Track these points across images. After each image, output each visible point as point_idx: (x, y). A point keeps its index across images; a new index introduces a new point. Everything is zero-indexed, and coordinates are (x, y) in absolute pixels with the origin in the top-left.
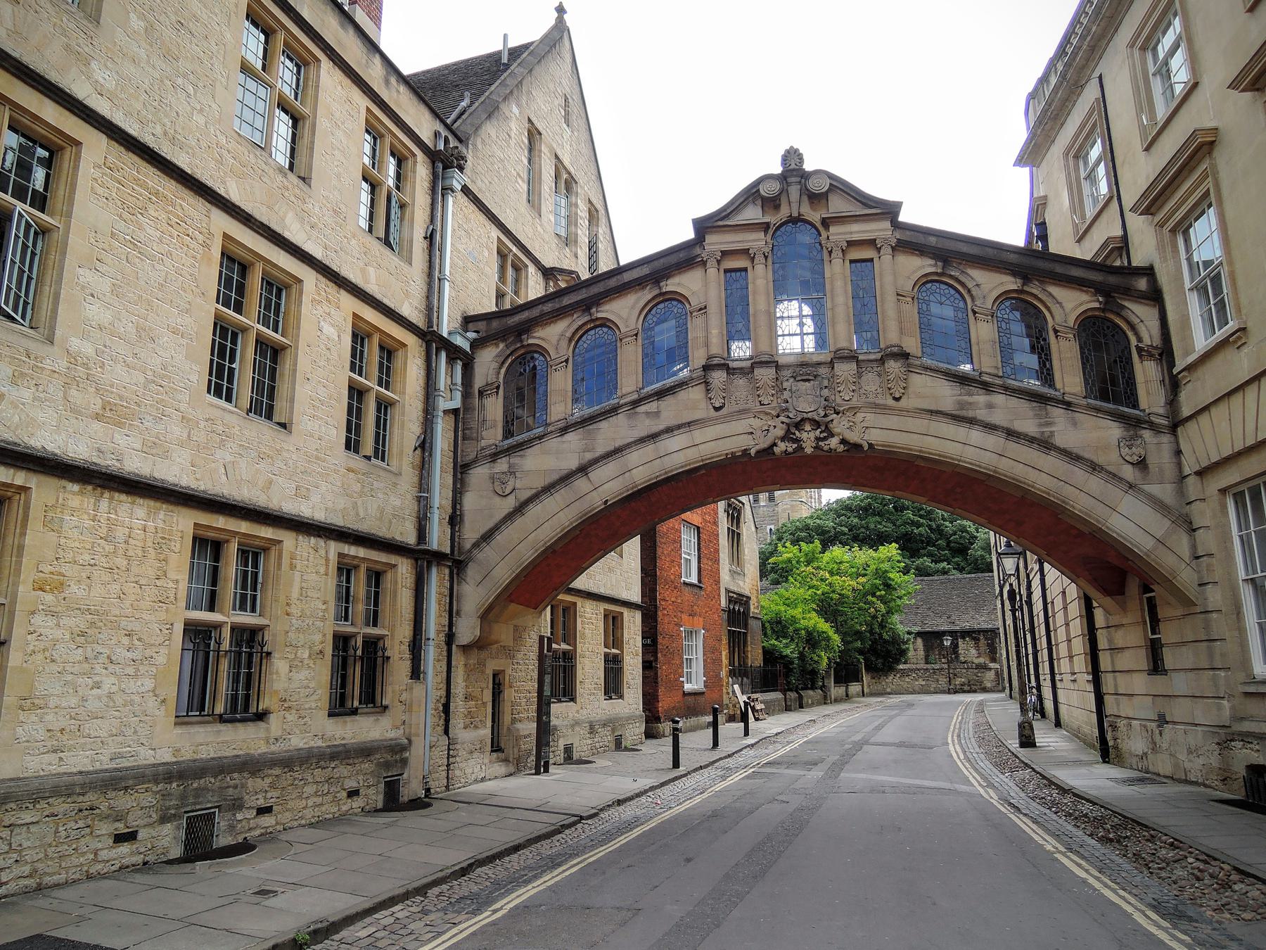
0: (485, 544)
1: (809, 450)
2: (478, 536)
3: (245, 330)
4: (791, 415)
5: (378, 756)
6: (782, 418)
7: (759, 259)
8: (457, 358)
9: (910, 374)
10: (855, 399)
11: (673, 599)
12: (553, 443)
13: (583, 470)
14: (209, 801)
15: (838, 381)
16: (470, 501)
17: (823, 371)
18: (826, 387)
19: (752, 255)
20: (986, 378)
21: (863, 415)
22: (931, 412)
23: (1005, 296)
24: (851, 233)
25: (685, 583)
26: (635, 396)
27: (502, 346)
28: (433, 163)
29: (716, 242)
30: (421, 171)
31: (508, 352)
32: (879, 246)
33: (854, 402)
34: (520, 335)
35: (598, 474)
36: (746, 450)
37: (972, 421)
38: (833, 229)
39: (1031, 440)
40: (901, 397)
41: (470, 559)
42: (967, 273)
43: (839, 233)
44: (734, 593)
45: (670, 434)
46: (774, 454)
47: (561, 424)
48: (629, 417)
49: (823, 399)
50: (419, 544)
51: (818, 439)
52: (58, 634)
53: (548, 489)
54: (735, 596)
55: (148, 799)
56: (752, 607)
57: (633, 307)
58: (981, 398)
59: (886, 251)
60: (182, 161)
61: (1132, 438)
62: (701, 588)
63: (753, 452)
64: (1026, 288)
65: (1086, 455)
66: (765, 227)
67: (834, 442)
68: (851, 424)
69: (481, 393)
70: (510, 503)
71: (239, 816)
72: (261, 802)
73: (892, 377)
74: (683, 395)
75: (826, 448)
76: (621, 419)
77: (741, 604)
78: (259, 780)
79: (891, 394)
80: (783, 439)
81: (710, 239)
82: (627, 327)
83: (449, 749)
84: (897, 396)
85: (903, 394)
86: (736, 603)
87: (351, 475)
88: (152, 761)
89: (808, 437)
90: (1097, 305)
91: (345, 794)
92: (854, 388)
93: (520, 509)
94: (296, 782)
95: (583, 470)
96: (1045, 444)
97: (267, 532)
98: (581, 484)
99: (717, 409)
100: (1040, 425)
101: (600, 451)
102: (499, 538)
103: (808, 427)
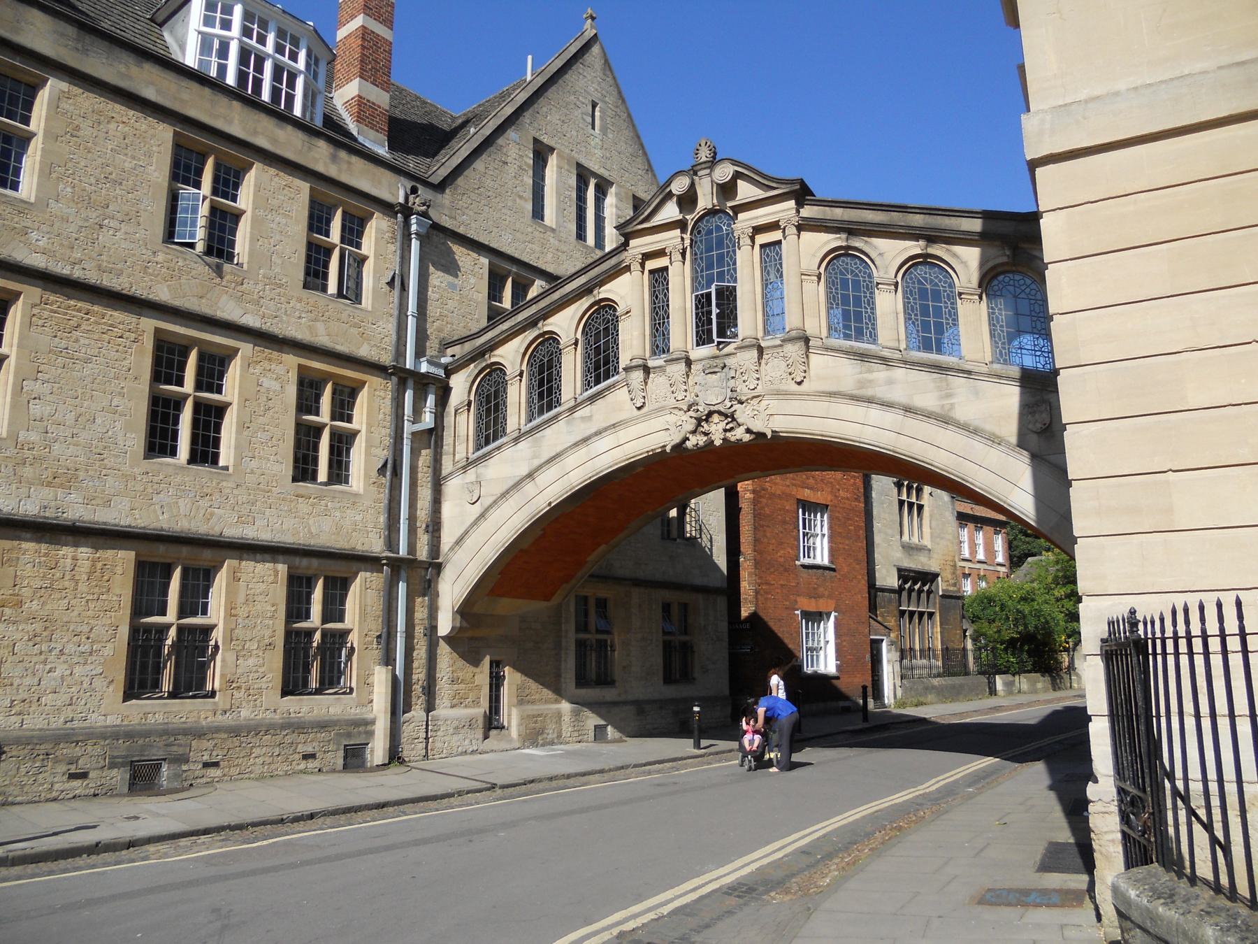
1: (718, 443)
2: (454, 540)
3: (186, 396)
4: (701, 409)
5: (337, 728)
6: (691, 413)
8: (429, 384)
11: (782, 582)
12: (509, 453)
13: (530, 476)
14: (156, 753)
16: (447, 510)
17: (729, 361)
18: (733, 378)
20: (886, 353)
21: (767, 402)
22: (831, 394)
23: (913, 263)
24: (757, 218)
25: (804, 566)
26: (572, 403)
27: (472, 366)
29: (639, 245)
31: (477, 371)
33: (759, 391)
34: (484, 355)
35: (543, 478)
36: (665, 446)
37: (870, 401)
38: (741, 216)
39: (928, 415)
41: (448, 561)
42: (870, 244)
43: (747, 220)
44: (910, 571)
45: (599, 437)
46: (686, 449)
47: (516, 434)
48: (568, 423)
49: (729, 390)
51: (725, 431)
52: (18, 636)
53: (504, 495)
55: (98, 750)
57: (572, 318)
58: (880, 373)
59: (794, 230)
60: (108, 282)
61: (1037, 404)
62: (833, 570)
63: (668, 449)
64: (931, 251)
65: (989, 427)
67: (739, 434)
68: (756, 412)
69: (456, 411)
70: (477, 510)
71: (185, 767)
72: (206, 758)
73: (791, 361)
74: (611, 398)
75: (733, 439)
76: (560, 426)
78: (205, 741)
80: (694, 432)
81: (633, 243)
82: (567, 337)
83: (427, 725)
84: (799, 380)
85: (805, 377)
86: (915, 583)
87: (300, 500)
88: (103, 724)
89: (716, 430)
90: (1005, 259)
91: (297, 756)
92: (757, 376)
93: (482, 516)
94: (244, 745)
95: (530, 476)
96: (945, 420)
97: (207, 555)
98: (529, 488)
99: (639, 408)
100: (941, 398)
101: (546, 456)
102: (468, 542)
103: (716, 418)
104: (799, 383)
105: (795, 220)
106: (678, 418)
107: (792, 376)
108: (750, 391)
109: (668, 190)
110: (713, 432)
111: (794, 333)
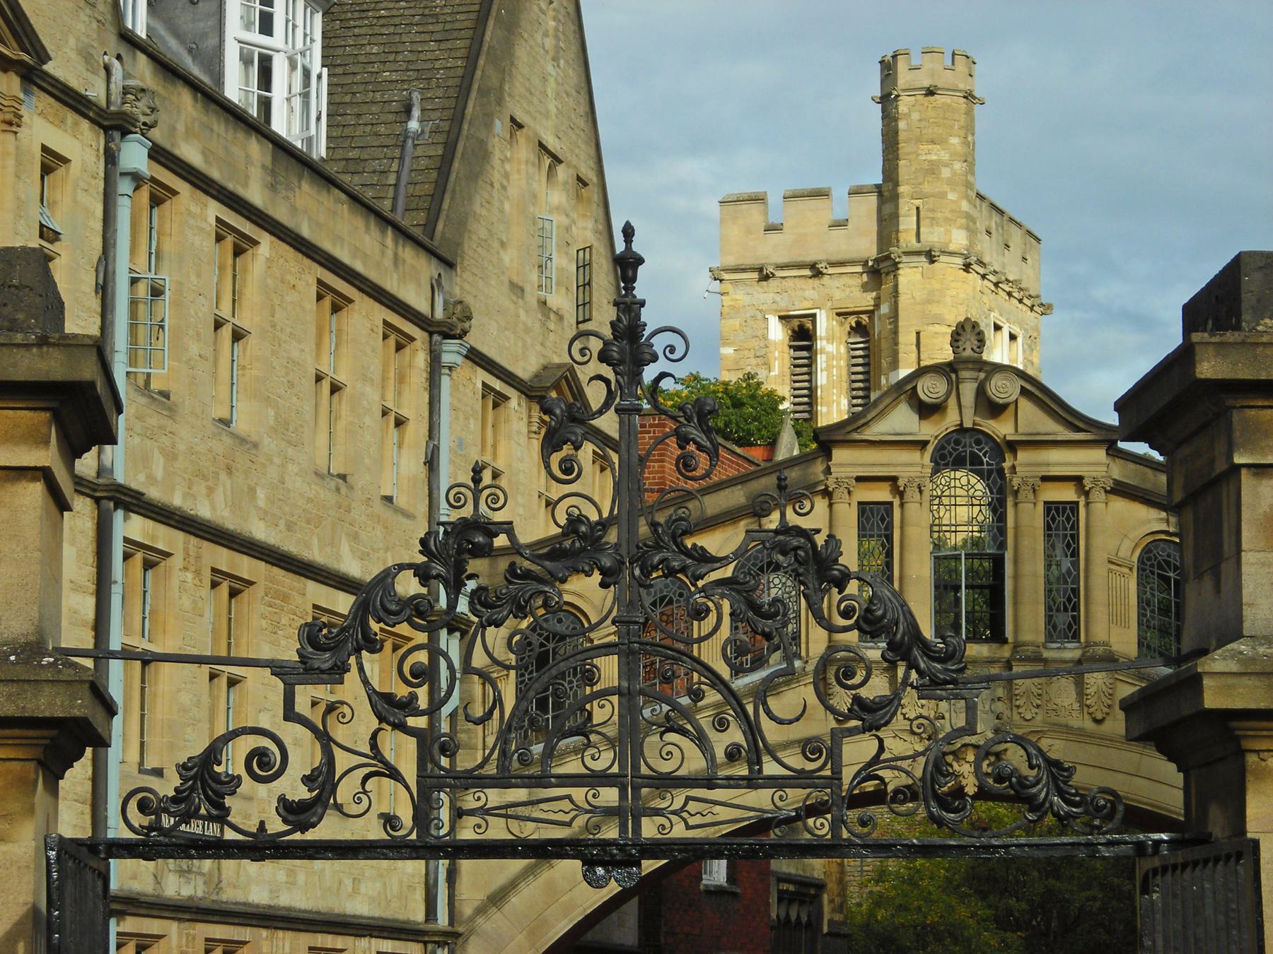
0: (494, 909)
2: (480, 896)
7: (912, 494)
9: (1119, 684)
10: (1039, 718)
15: (1017, 692)
18: (999, 699)
19: (902, 489)
21: (1049, 741)
24: (1048, 465)
28: (431, 334)
30: (419, 358)
32: (1087, 488)
38: (1023, 456)
40: (1104, 719)
41: (472, 932)
49: (992, 717)
50: (427, 920)
54: (792, 888)
56: (826, 908)
62: (734, 894)
66: (923, 444)
77: (802, 903)
79: (1090, 714)
81: (839, 455)
84: (1099, 717)
85: (1107, 714)
86: (791, 902)
92: (1039, 702)
104: (1098, 722)
105: (1109, 484)
106: (907, 745)
107: (1091, 710)
108: (1026, 723)
109: (909, 387)
110: (966, 774)
111: (1100, 650)
